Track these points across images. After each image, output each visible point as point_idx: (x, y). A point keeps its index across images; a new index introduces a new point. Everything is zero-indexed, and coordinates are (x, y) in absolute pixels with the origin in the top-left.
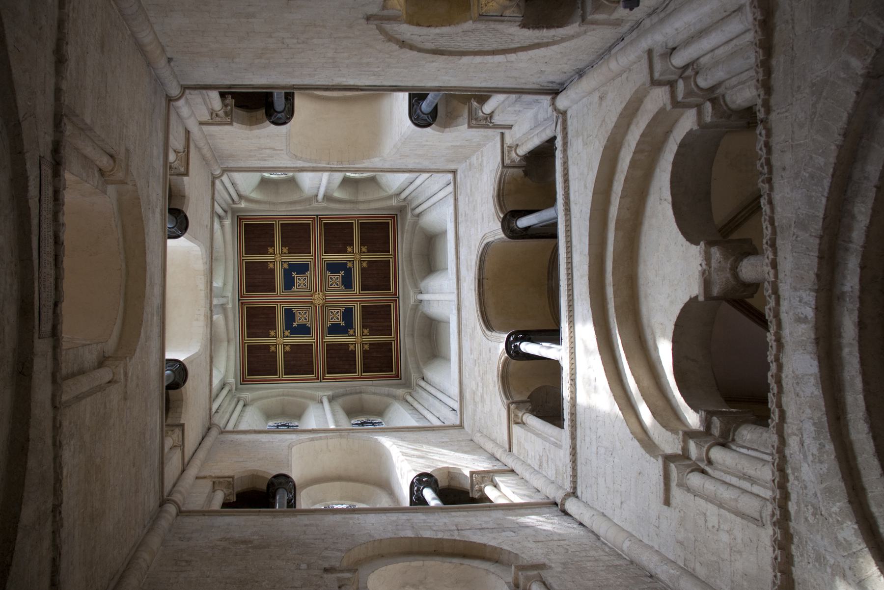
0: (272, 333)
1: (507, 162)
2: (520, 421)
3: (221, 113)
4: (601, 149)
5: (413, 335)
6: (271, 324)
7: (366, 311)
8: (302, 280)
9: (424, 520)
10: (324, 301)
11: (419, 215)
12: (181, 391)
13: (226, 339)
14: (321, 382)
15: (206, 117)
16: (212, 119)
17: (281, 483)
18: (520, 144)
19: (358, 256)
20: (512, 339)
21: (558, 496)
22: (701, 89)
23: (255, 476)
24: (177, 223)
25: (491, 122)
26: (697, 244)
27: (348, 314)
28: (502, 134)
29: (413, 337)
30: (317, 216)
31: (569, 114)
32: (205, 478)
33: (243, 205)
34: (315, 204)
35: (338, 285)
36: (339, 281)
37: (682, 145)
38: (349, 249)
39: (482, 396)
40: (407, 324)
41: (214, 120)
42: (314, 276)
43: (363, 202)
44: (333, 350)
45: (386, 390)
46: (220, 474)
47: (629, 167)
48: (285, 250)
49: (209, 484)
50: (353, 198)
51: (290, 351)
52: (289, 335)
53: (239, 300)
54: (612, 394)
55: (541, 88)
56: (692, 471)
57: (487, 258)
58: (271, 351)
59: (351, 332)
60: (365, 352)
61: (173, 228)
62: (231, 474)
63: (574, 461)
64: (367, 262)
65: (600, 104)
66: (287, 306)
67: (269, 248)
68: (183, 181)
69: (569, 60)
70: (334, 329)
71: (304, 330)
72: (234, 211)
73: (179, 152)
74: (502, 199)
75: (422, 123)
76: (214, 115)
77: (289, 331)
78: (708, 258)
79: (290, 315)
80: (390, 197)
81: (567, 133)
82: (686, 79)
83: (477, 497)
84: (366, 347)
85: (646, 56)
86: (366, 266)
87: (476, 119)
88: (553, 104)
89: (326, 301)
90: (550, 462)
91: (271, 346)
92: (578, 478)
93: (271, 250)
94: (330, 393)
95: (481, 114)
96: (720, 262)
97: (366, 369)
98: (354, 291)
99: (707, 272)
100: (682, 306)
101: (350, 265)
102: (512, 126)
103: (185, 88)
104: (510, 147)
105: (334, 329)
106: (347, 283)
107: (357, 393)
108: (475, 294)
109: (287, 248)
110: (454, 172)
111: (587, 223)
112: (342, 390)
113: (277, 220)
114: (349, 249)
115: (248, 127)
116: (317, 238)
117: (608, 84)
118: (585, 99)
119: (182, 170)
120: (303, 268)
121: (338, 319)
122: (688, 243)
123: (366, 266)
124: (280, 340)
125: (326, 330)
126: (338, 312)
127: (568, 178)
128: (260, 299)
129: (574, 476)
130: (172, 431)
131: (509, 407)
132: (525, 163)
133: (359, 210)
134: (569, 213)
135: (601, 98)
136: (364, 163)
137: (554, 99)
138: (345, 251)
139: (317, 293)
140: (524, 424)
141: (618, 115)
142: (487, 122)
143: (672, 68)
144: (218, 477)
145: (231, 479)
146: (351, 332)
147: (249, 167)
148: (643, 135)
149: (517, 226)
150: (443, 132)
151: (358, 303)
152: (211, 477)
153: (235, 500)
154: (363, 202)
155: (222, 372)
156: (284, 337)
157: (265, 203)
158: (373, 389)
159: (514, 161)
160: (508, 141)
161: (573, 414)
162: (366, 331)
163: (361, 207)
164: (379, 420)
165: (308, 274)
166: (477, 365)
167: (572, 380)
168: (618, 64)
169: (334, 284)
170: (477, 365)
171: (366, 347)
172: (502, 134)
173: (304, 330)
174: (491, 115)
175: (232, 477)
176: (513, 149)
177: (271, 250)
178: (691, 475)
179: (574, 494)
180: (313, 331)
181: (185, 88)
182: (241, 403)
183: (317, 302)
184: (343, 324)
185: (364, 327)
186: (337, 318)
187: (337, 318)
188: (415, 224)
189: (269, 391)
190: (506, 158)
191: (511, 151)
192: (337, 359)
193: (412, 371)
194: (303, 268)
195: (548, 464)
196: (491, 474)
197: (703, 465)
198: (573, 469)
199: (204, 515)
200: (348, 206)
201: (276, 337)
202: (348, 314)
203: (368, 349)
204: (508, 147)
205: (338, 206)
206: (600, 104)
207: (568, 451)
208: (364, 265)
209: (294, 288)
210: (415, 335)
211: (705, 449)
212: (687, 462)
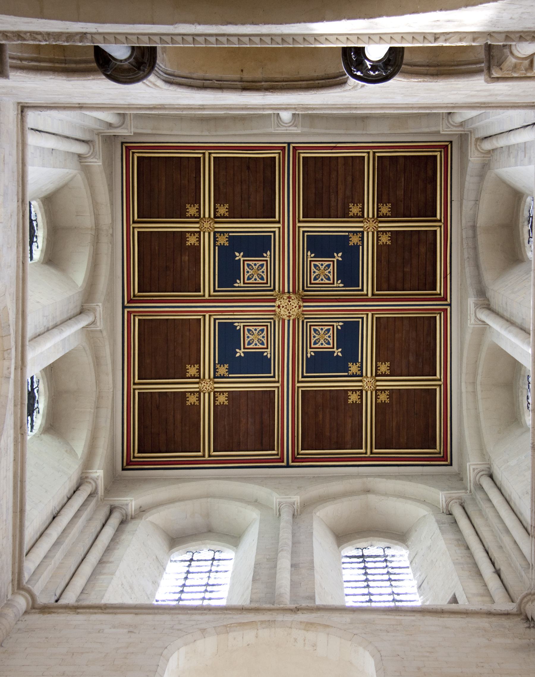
8: (251, 337)
10: (293, 296)
14: (450, 305)
35: (262, 265)
36: (255, 262)
38: (192, 240)
45: (470, 181)
51: (388, 364)
52: (359, 365)
53: (288, 466)
58: (388, 401)
67: (188, 403)
77: (350, 365)
86: (227, 206)
89: (294, 292)
91: (379, 401)
98: (274, 232)
109: (188, 366)
114: (192, 240)
121: (329, 266)
123: (227, 206)
125: (350, 291)
126: (315, 266)
138: (196, 250)
139: (278, 310)
151: (298, 225)
155: (426, 513)
156: (361, 376)
158: (468, 205)
162: (355, 210)
165: (239, 326)
169: (260, 272)
183: (295, 312)
184: (338, 257)
185: (345, 214)
192: (407, 269)
203: (389, 205)
209: (268, 353)
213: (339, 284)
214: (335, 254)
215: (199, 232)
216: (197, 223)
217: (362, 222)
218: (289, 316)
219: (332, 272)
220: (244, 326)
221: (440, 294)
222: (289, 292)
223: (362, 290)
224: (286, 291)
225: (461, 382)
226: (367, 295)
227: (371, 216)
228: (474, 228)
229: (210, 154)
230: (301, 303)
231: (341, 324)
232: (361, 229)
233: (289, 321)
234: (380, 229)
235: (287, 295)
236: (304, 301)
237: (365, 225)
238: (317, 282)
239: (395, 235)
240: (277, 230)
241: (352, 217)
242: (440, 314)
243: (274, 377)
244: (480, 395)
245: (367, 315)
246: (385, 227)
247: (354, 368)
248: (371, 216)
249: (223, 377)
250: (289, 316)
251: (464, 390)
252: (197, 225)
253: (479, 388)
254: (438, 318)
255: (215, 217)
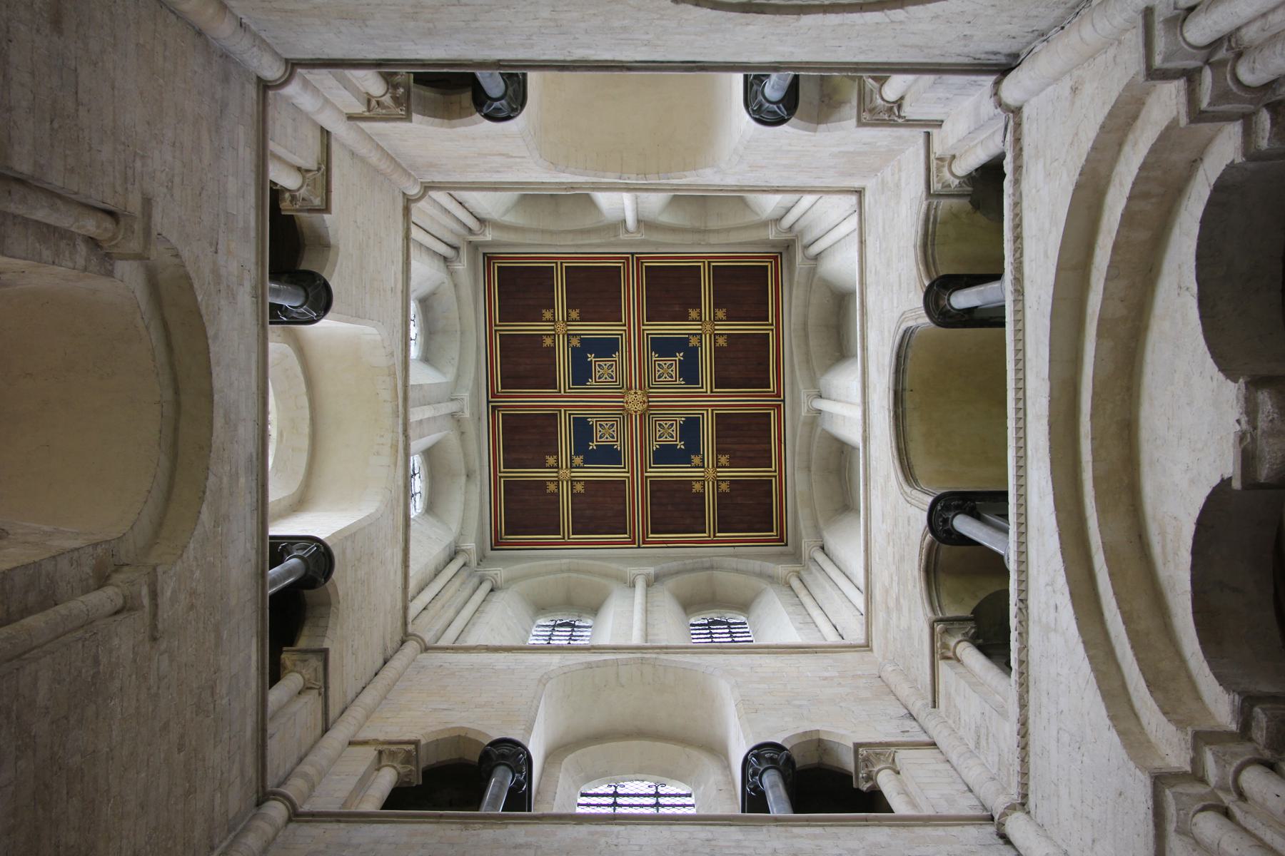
0: (551, 460)
1: (936, 186)
2: (950, 654)
3: (387, 100)
4: (1071, 189)
5: (809, 469)
6: (551, 446)
7: (725, 424)
9: (739, 841)
10: (645, 406)
11: (817, 257)
12: (326, 589)
13: (463, 471)
14: (639, 547)
15: (360, 108)
16: (369, 110)
17: (503, 756)
18: (957, 155)
19: (708, 327)
20: (939, 508)
21: (998, 804)
22: (1247, 88)
23: (460, 739)
24: (307, 297)
25: (899, 116)
26: (1235, 381)
27: (690, 428)
28: (928, 135)
29: (809, 470)
30: (633, 254)
31: (1026, 112)
32: (365, 743)
33: (489, 236)
34: (623, 237)
36: (674, 371)
37: (1220, 188)
38: (693, 314)
39: (898, 600)
40: (797, 449)
41: (373, 110)
42: (627, 360)
43: (717, 231)
44: (660, 489)
46: (394, 737)
47: (1121, 225)
48: (574, 314)
49: (371, 752)
50: (697, 224)
51: (583, 491)
52: (582, 465)
53: (488, 402)
54: (1080, 640)
55: (976, 62)
56: (1204, 809)
57: (910, 354)
58: (548, 491)
59: (696, 460)
60: (721, 497)
61: (301, 306)
62: (412, 737)
63: (1024, 747)
64: (725, 337)
65: (1073, 103)
66: (579, 413)
67: (544, 311)
68: (324, 221)
69: (1012, 17)
70: (665, 455)
71: (609, 455)
72: (474, 246)
73: (308, 171)
74: (930, 252)
75: (769, 117)
76: (374, 103)
77: (581, 457)
78: (1251, 410)
79: (583, 429)
80: (765, 224)
81: (1021, 149)
82: (1217, 66)
83: (865, 789)
84: (724, 487)
85: (1140, 22)
86: (725, 345)
87: (872, 111)
88: (996, 94)
89: (649, 406)
90: (991, 740)
91: (548, 483)
92: (1031, 778)
93: (548, 315)
94: (651, 570)
95: (879, 101)
96: (1271, 421)
97: (724, 525)
98: (702, 388)
99: (1249, 435)
100: (1207, 491)
101: (694, 342)
102: (942, 121)
103: (293, 66)
104: (941, 159)
105: (665, 455)
106: (689, 373)
107: (707, 569)
108: (889, 416)
109: (578, 311)
110: (859, 193)
111: (1047, 322)
112: (675, 563)
113: (559, 262)
114: (693, 314)
115: (446, 121)
116: (632, 294)
117: (1086, 65)
118: (1050, 88)
119: (317, 202)
120: (607, 347)
121: (672, 437)
122: (1221, 376)
123: (725, 345)
124: (565, 473)
125: (649, 457)
126: (672, 425)
127: (1021, 233)
128: (530, 401)
129: (1024, 774)
130: (305, 661)
131: (932, 629)
132: (970, 189)
133: (709, 245)
134: (1021, 298)
135: (1074, 90)
136: (686, 177)
137: (997, 84)
138: (684, 317)
139: (633, 392)
140: (959, 660)
141: (1098, 127)
142: (891, 115)
143: (1186, 47)
144: (390, 743)
145: (411, 747)
146: (696, 460)
147: (473, 183)
148: (1143, 168)
149: (950, 304)
150: (815, 131)
151: (710, 409)
152: (376, 742)
153: (421, 783)
154: (717, 231)
156: (572, 467)
157: (535, 231)
158: (733, 562)
159: (949, 186)
160: (937, 149)
161: (1024, 662)
162: (724, 459)
163: (713, 239)
164: (742, 619)
165: (616, 356)
166: (891, 543)
167: (1021, 600)
168: (1096, 31)
169: (666, 375)
170: (891, 543)
171: (724, 487)
172: (928, 135)
173: (609, 455)
174: (899, 103)
175: (416, 743)
176: (946, 164)
177: (548, 315)
178: (1200, 816)
179: (1022, 804)
180: (626, 457)
181: (293, 66)
182: (486, 587)
183: (632, 407)
184: (681, 445)
185: (720, 451)
186: (671, 436)
187: (671, 436)
188: (812, 272)
189: (543, 563)
190: (934, 179)
191: (943, 166)
192: (670, 508)
193: (804, 533)
194: (607, 347)
195: (988, 743)
196: (893, 749)
197: (1228, 799)
198: (1023, 761)
199: (339, 821)
200: (689, 238)
201: (557, 467)
202: (690, 428)
203: (728, 491)
204: (937, 159)
205: (669, 238)
206: (1073, 103)
207: (1016, 727)
208: (722, 342)
209: (591, 382)
210: (813, 468)
211: (1231, 770)
212: (1199, 789)
213: (656, 446)
214: (683, 443)
215: (701, 320)
216: (710, 319)
217: (713, 466)
218: (627, 403)
219: (666, 440)
220: (616, 361)
221: (648, 538)
222: (649, 402)
223: (650, 467)
224: (650, 399)
225: (569, 558)
226: (646, 472)
227: (719, 474)
228: (712, 568)
229: (772, 330)
230: (639, 413)
231: (619, 448)
232: (706, 466)
233: (622, 402)
234: (706, 483)
235: (646, 401)
236: (641, 416)
237: (711, 470)
238: (658, 426)
239: (701, 496)
240: (704, 390)
241: (717, 456)
242: (630, 538)
243: (569, 388)
244: (559, 576)
245: (628, 472)
246: (709, 488)
247: (578, 460)
248: (719, 474)
249: (568, 343)
250: (627, 403)
251: (564, 561)
252: (707, 319)
253: (565, 575)
254: (626, 536)
255: (715, 335)
